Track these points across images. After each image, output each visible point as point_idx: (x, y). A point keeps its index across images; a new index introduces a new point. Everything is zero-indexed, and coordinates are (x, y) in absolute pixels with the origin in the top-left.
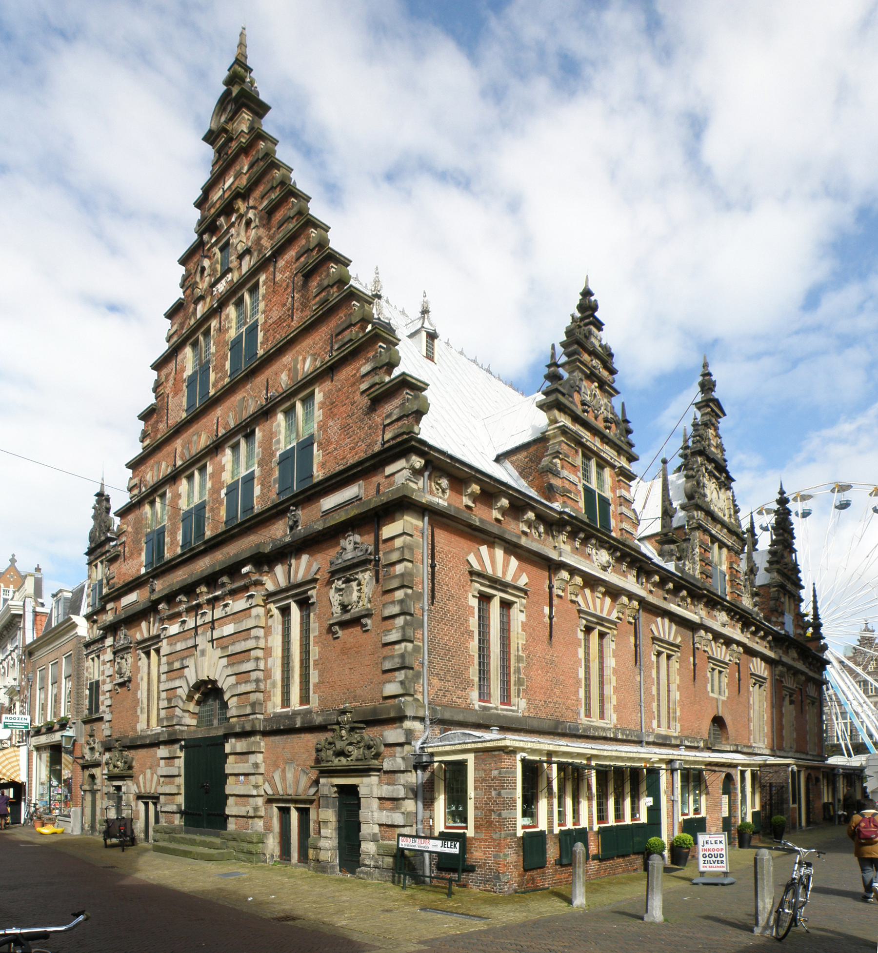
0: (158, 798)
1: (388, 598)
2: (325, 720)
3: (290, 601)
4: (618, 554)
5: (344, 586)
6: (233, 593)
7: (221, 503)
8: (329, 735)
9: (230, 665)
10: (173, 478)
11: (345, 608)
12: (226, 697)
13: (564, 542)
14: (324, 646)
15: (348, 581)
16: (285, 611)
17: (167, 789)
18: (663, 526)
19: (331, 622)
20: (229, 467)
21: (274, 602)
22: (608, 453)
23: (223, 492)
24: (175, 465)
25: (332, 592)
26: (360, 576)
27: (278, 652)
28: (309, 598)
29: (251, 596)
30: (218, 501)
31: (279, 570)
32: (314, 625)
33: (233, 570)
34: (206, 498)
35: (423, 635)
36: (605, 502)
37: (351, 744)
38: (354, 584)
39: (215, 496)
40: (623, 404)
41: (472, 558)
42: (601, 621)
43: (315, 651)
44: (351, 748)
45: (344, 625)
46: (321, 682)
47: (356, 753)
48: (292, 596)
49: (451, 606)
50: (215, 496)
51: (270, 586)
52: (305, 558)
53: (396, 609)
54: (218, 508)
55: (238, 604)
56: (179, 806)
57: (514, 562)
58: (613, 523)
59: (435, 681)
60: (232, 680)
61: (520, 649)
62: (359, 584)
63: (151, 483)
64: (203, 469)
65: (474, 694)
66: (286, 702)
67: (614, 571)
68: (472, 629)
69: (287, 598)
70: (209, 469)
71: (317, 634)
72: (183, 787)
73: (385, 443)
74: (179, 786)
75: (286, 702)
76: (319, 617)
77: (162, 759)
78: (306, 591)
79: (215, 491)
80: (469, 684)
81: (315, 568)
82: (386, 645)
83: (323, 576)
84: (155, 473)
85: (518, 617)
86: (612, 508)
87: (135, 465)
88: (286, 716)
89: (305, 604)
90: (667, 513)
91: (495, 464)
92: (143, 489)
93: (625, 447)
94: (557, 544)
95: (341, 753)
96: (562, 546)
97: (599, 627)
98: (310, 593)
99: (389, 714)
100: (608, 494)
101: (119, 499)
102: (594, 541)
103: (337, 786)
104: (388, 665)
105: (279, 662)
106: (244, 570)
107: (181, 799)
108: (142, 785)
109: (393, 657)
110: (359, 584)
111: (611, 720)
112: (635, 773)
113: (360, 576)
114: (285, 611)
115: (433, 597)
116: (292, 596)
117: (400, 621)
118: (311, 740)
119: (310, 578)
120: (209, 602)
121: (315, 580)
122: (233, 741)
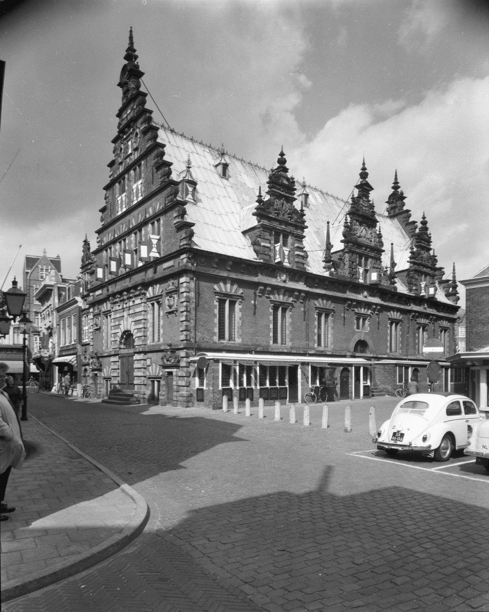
0: (110, 378)
1: (181, 305)
4: (292, 274)
6: (136, 296)
8: (164, 353)
9: (135, 325)
10: (114, 242)
11: (170, 307)
12: (134, 337)
14: (164, 319)
16: (153, 305)
17: (115, 374)
20: (134, 242)
21: (150, 301)
22: (289, 229)
24: (114, 236)
25: (166, 300)
26: (173, 296)
27: (151, 321)
28: (159, 302)
29: (141, 299)
31: (150, 289)
33: (135, 287)
37: (170, 357)
38: (172, 298)
42: (282, 303)
43: (161, 323)
44: (170, 359)
45: (170, 313)
46: (163, 334)
47: (172, 361)
48: (155, 300)
49: (206, 306)
51: (148, 295)
52: (158, 285)
53: (183, 309)
55: (138, 301)
56: (119, 381)
57: (235, 286)
62: (174, 299)
63: (105, 242)
64: (125, 240)
65: (216, 338)
66: (153, 341)
68: (216, 313)
69: (154, 300)
72: (120, 374)
73: (180, 246)
74: (118, 373)
75: (153, 341)
77: (113, 362)
78: (158, 299)
80: (214, 334)
81: (161, 291)
83: (164, 293)
84: (107, 238)
85: (238, 307)
87: (99, 232)
88: (153, 346)
89: (158, 303)
91: (242, 234)
92: (103, 244)
93: (299, 224)
95: (167, 361)
98: (160, 300)
101: (94, 246)
102: (277, 271)
105: (151, 325)
106: (139, 288)
107: (119, 379)
108: (105, 373)
110: (174, 299)
111: (289, 344)
112: (282, 369)
113: (173, 296)
114: (153, 305)
116: (155, 300)
117: (185, 313)
118: (161, 355)
119: (159, 294)
121: (161, 295)
122: (136, 355)
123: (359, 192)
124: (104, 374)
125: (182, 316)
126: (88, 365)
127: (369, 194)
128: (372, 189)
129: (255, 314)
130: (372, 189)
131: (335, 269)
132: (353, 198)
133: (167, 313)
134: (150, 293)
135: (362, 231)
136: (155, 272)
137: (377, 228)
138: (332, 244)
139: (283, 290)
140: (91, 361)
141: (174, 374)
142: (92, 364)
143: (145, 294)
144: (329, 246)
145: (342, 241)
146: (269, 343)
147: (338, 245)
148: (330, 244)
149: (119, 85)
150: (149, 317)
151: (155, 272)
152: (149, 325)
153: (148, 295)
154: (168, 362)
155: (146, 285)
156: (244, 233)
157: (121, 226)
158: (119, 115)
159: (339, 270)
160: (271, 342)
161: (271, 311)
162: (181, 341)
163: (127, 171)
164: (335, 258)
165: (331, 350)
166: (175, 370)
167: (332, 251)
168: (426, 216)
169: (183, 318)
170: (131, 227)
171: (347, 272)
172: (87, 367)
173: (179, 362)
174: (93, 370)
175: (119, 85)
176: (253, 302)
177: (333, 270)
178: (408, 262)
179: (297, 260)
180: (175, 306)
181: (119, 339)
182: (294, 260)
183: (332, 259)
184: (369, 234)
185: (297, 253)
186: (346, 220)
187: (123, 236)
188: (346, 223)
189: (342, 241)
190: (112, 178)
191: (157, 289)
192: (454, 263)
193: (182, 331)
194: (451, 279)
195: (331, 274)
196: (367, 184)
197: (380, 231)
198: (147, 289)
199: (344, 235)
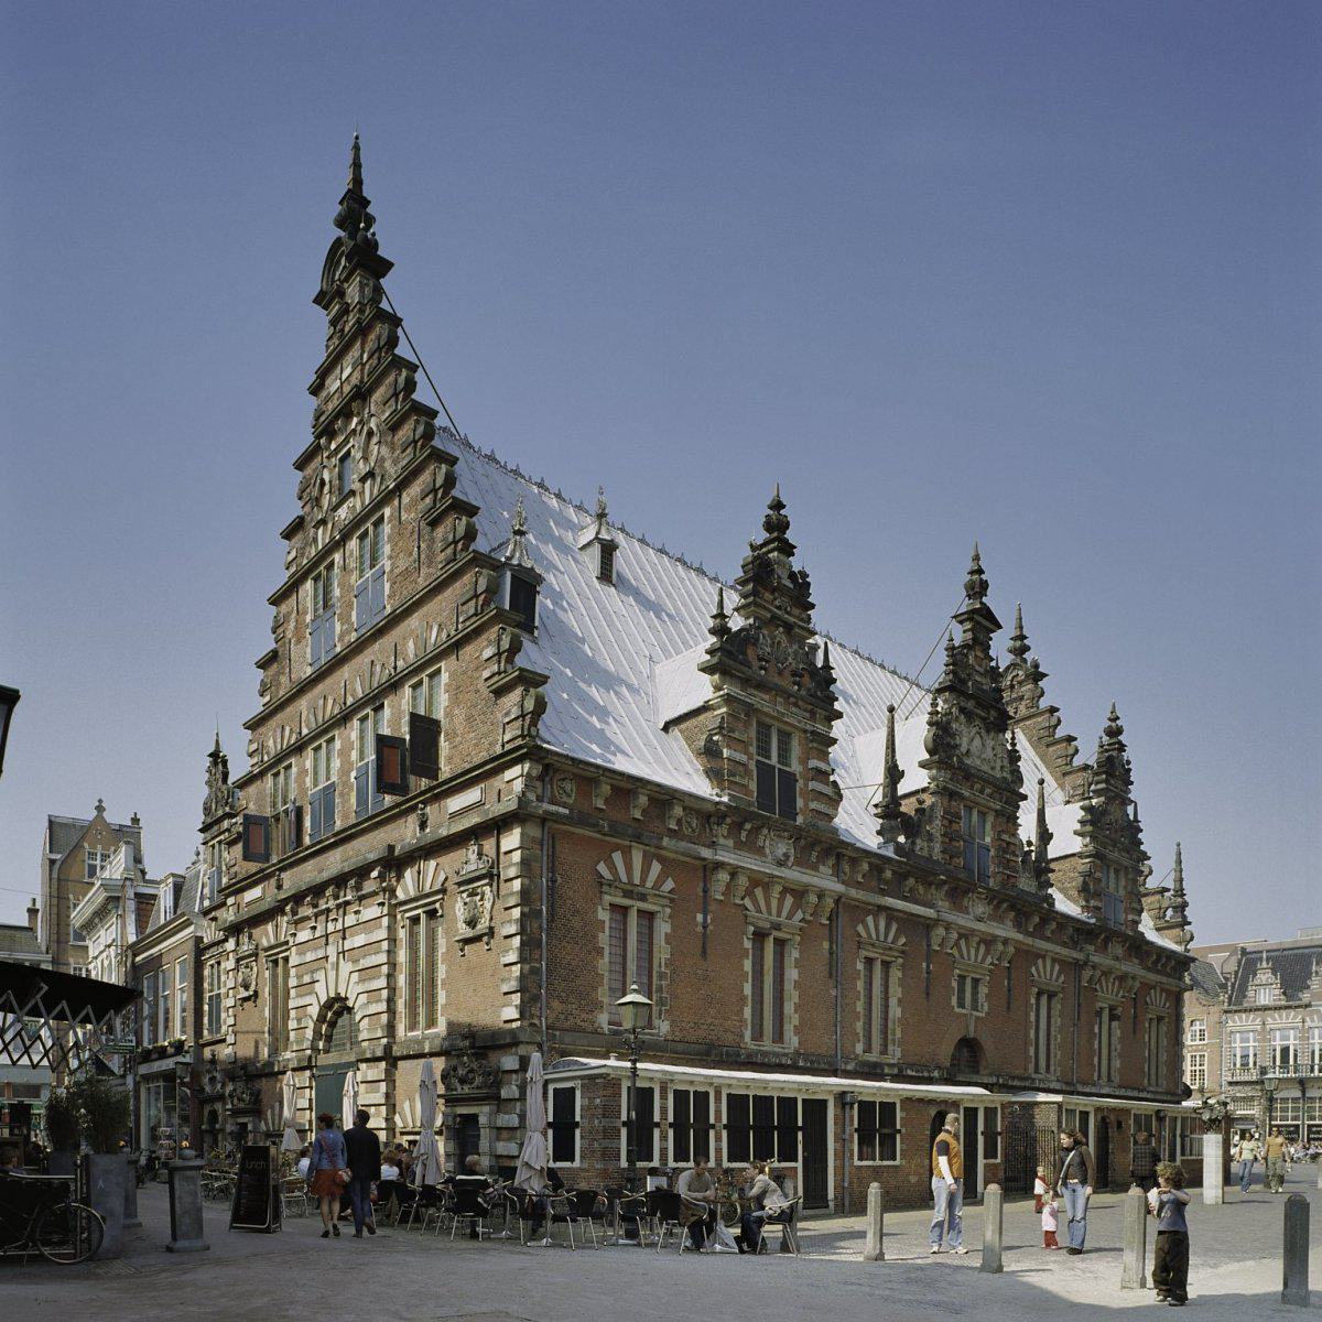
2: (451, 1045)
3: (420, 911)
5: (468, 900)
6: (361, 899)
7: (351, 789)
11: (472, 923)
13: (725, 837)
15: (473, 894)
18: (885, 796)
19: (456, 939)
20: (357, 745)
23: (353, 774)
25: (459, 905)
30: (346, 784)
31: (409, 874)
32: (442, 943)
33: (362, 872)
34: (334, 778)
35: (541, 956)
36: (789, 780)
37: (471, 1071)
38: (479, 897)
39: (344, 779)
41: (602, 868)
43: (442, 971)
45: (467, 941)
47: (478, 1080)
49: (576, 923)
50: (344, 779)
52: (432, 863)
54: (349, 795)
58: (800, 803)
59: (556, 1004)
60: (363, 998)
61: (663, 964)
67: (798, 863)
69: (417, 908)
70: (338, 744)
71: (444, 950)
76: (446, 932)
78: (434, 902)
79: (345, 772)
82: (506, 965)
86: (800, 784)
90: (894, 774)
94: (715, 840)
95: (462, 1081)
96: (721, 841)
97: (775, 933)
98: (437, 905)
99: (505, 1039)
100: (795, 767)
103: (460, 1115)
104: (505, 988)
106: (374, 874)
109: (509, 979)
115: (553, 915)
120: (338, 906)
121: (443, 891)
123: (964, 632)
124: (267, 1124)
125: (507, 951)
126: (221, 1098)
127: (991, 639)
128: (1000, 627)
129: (704, 953)
130: (1000, 627)
131: (907, 838)
132: (951, 649)
133: (458, 941)
134: (407, 886)
135: (970, 740)
136: (423, 825)
137: (1008, 735)
138: (901, 768)
139: (778, 888)
140: (230, 1088)
141: (483, 1120)
142: (231, 1096)
143: (393, 892)
144: (894, 774)
145: (923, 765)
147: (915, 779)
148: (896, 766)
149: (317, 301)
150: (402, 956)
151: (423, 825)
152: (402, 980)
153: (401, 895)
154: (466, 1087)
155: (394, 863)
156: (666, 728)
157: (321, 702)
158: (316, 390)
159: (918, 841)
160: (748, 1034)
161: (748, 944)
162: (506, 1022)
163: (338, 544)
164: (908, 807)
165: (895, 1061)
166: (486, 1109)
167: (902, 789)
169: (512, 957)
170: (350, 701)
171: (937, 847)
172: (218, 1106)
173: (498, 1085)
174: (236, 1113)
175: (317, 301)
176: (700, 917)
177: (901, 839)
178: (1076, 833)
179: (814, 805)
180: (483, 926)
181: (311, 1025)
182: (806, 805)
183: (902, 809)
184: (989, 750)
185: (812, 785)
186: (934, 705)
187: (325, 731)
188: (934, 713)
189: (923, 765)
190: (293, 569)
191: (433, 872)
192: (1179, 845)
193: (506, 994)
194: (1170, 884)
195: (899, 849)
196: (987, 613)
197: (1014, 745)
198: (400, 877)
199: (931, 752)
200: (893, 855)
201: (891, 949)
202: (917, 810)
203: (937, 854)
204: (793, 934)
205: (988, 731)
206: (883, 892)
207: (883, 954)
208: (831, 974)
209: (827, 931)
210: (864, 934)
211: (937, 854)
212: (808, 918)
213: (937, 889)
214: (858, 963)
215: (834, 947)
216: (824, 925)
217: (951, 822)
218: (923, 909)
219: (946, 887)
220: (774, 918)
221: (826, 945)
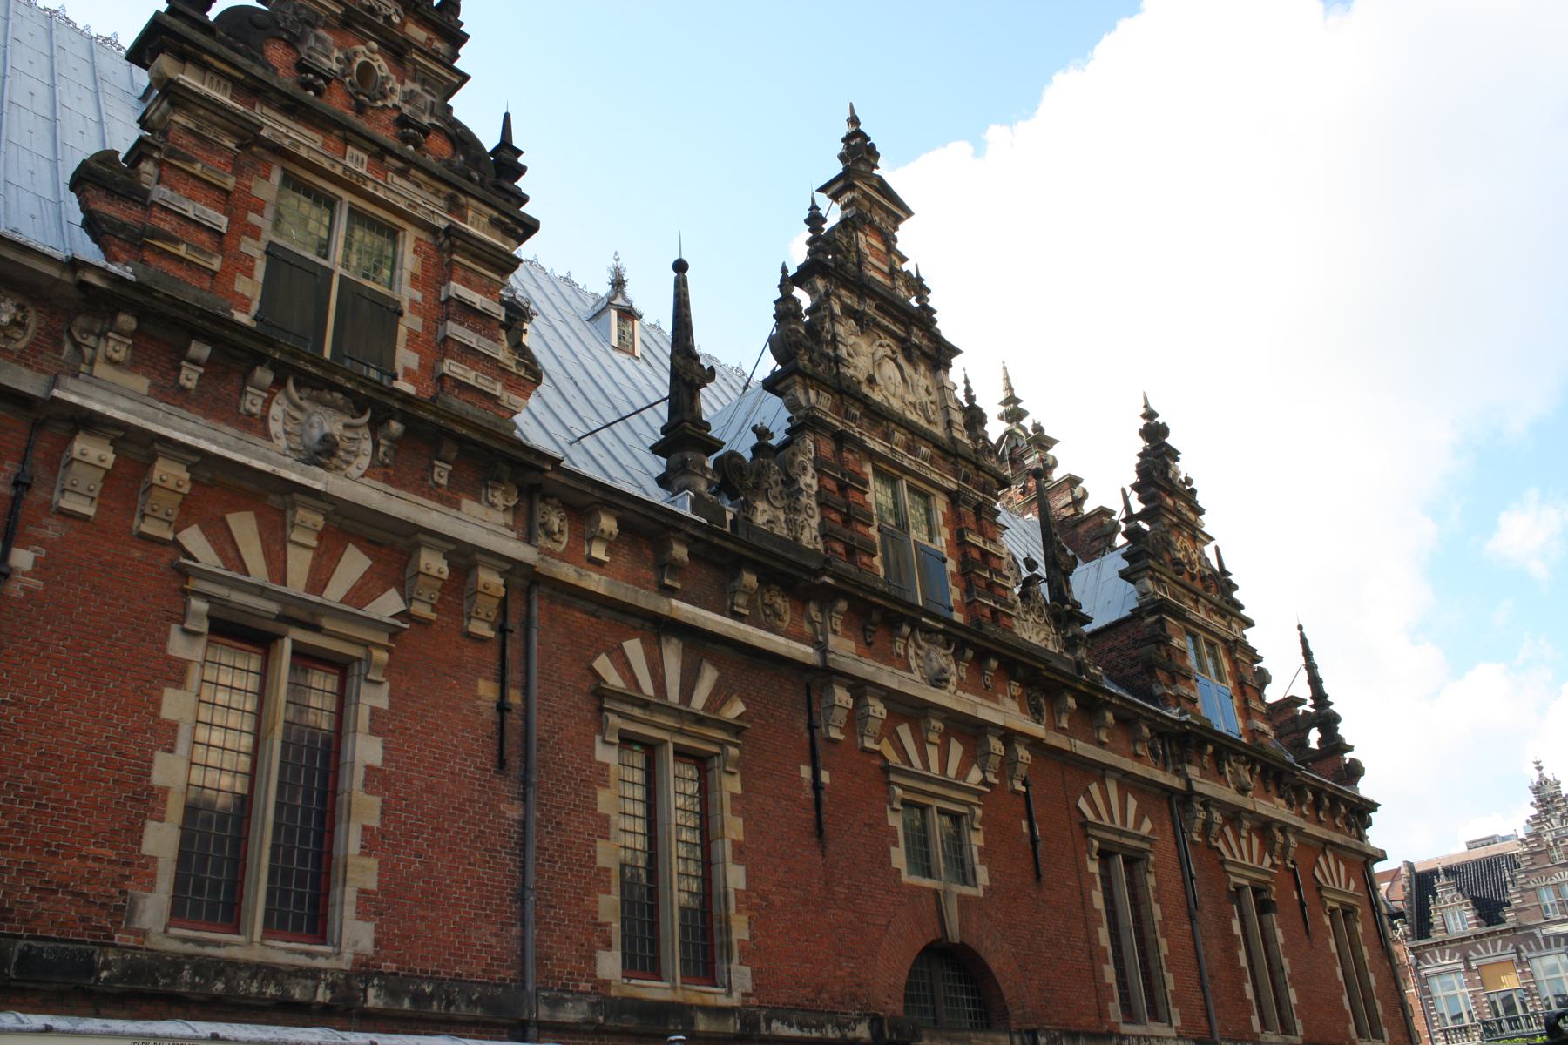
40: (507, 118)
146: (123, 911)
168: (1154, 406)
200: (687, 513)
201: (700, 720)
202: (755, 449)
203: (809, 536)
204: (367, 645)
205: (909, 359)
206: (669, 592)
207: (680, 732)
208: (502, 764)
209: (491, 655)
210: (614, 679)
211: (809, 536)
212: (422, 610)
213: (821, 611)
214: (599, 746)
215: (515, 697)
216: (483, 640)
217: (843, 487)
218: (781, 640)
219: (842, 605)
220: (296, 584)
221: (487, 690)
